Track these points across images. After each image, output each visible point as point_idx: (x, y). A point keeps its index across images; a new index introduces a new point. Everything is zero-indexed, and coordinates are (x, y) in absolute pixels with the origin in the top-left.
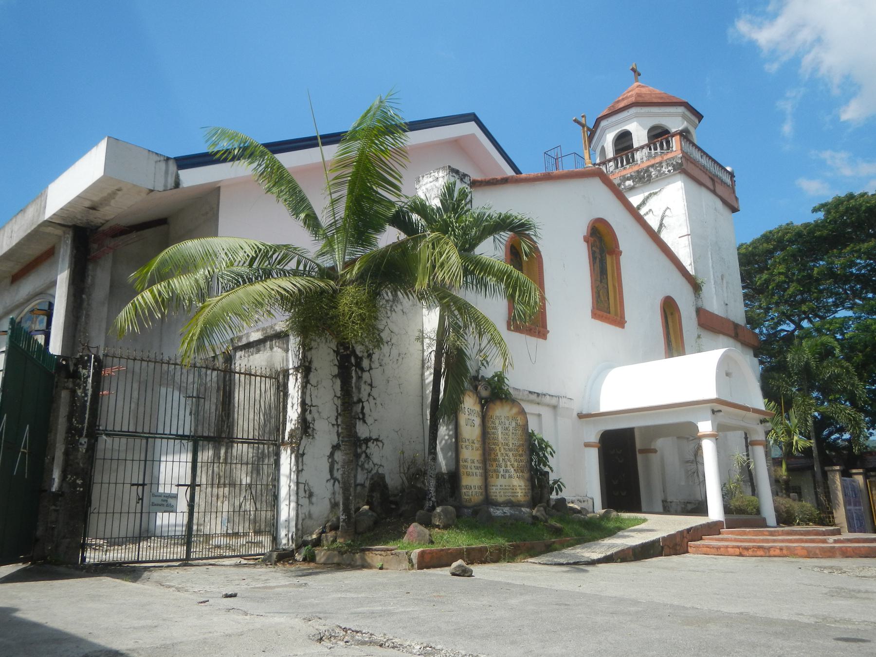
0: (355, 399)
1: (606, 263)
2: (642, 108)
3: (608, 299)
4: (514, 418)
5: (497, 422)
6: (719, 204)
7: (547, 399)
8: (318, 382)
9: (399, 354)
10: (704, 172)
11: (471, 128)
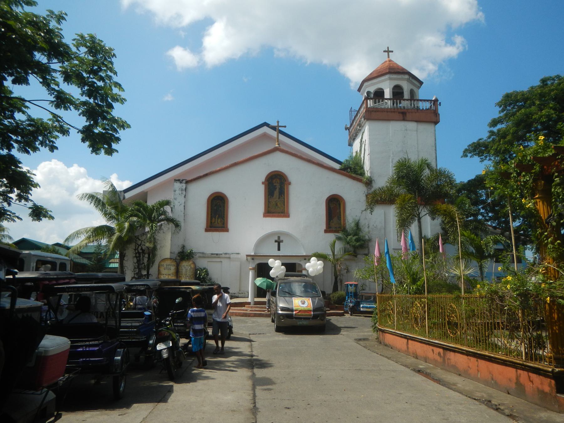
0: (142, 263)
1: (284, 189)
3: (284, 205)
4: (190, 265)
5: (183, 268)
7: (223, 255)
8: (127, 260)
9: (161, 247)
10: (391, 112)
11: (265, 129)
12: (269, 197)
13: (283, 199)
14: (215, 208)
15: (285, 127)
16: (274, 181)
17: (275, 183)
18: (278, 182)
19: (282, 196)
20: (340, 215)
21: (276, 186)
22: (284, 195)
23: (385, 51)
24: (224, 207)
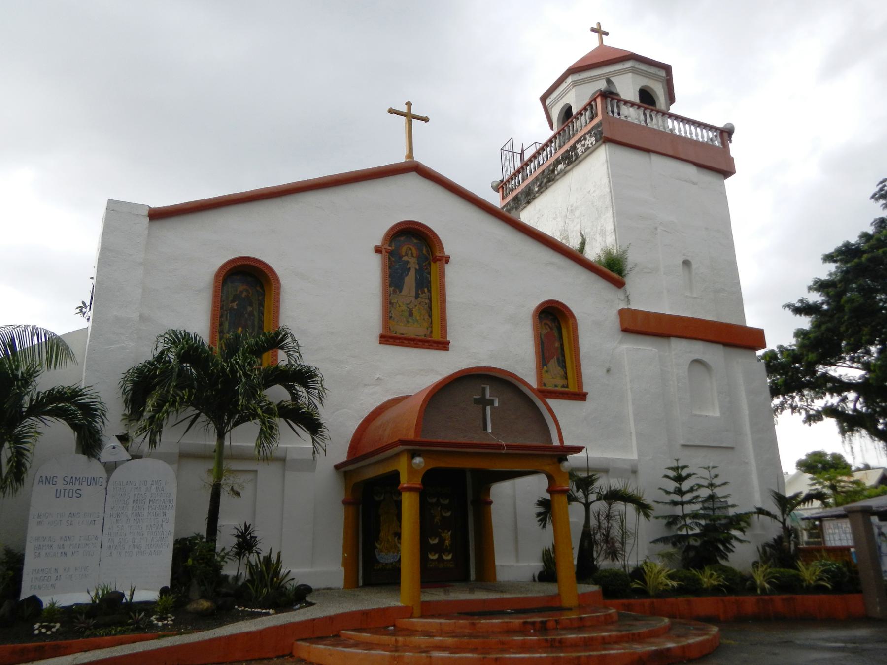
1: (429, 273)
2: (580, 74)
3: (431, 316)
6: (691, 171)
12: (392, 289)
13: (427, 301)
14: (235, 305)
15: (426, 120)
16: (404, 250)
17: (406, 255)
18: (412, 254)
19: (423, 292)
20: (563, 355)
21: (408, 262)
22: (430, 291)
23: (593, 30)
24: (261, 305)
